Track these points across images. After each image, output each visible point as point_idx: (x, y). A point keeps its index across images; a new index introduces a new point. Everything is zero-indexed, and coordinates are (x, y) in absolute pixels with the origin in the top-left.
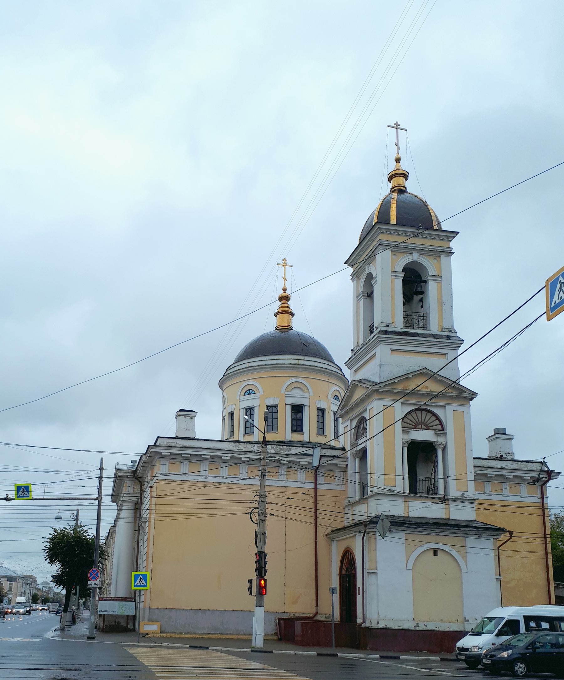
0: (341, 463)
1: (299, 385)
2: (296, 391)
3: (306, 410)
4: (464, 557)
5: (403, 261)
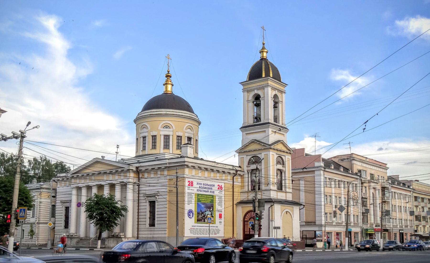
0: (241, 173)
1: (191, 128)
2: (189, 130)
3: (192, 139)
4: (293, 214)
5: (274, 93)
